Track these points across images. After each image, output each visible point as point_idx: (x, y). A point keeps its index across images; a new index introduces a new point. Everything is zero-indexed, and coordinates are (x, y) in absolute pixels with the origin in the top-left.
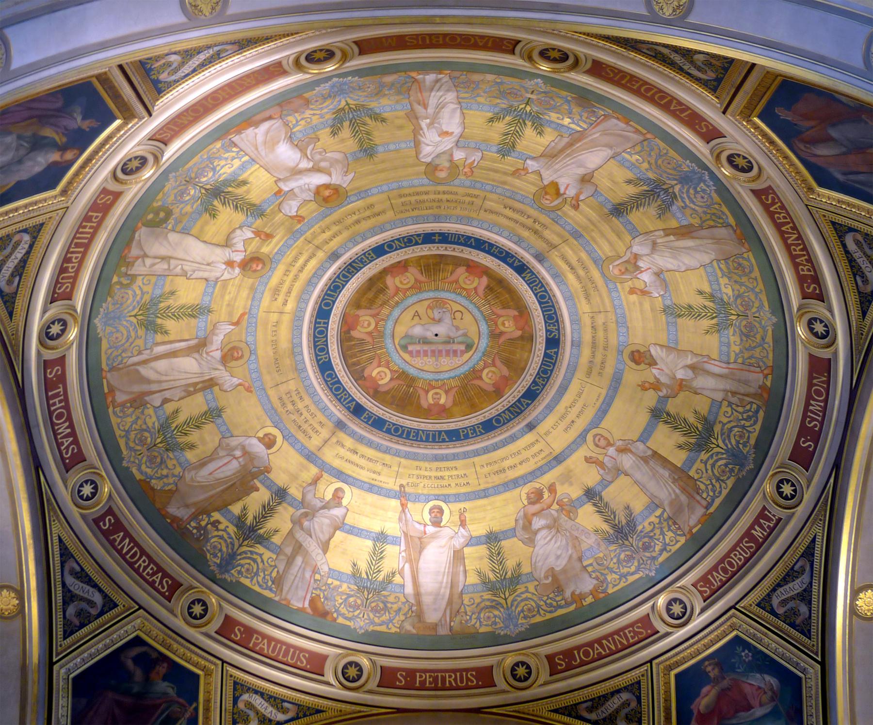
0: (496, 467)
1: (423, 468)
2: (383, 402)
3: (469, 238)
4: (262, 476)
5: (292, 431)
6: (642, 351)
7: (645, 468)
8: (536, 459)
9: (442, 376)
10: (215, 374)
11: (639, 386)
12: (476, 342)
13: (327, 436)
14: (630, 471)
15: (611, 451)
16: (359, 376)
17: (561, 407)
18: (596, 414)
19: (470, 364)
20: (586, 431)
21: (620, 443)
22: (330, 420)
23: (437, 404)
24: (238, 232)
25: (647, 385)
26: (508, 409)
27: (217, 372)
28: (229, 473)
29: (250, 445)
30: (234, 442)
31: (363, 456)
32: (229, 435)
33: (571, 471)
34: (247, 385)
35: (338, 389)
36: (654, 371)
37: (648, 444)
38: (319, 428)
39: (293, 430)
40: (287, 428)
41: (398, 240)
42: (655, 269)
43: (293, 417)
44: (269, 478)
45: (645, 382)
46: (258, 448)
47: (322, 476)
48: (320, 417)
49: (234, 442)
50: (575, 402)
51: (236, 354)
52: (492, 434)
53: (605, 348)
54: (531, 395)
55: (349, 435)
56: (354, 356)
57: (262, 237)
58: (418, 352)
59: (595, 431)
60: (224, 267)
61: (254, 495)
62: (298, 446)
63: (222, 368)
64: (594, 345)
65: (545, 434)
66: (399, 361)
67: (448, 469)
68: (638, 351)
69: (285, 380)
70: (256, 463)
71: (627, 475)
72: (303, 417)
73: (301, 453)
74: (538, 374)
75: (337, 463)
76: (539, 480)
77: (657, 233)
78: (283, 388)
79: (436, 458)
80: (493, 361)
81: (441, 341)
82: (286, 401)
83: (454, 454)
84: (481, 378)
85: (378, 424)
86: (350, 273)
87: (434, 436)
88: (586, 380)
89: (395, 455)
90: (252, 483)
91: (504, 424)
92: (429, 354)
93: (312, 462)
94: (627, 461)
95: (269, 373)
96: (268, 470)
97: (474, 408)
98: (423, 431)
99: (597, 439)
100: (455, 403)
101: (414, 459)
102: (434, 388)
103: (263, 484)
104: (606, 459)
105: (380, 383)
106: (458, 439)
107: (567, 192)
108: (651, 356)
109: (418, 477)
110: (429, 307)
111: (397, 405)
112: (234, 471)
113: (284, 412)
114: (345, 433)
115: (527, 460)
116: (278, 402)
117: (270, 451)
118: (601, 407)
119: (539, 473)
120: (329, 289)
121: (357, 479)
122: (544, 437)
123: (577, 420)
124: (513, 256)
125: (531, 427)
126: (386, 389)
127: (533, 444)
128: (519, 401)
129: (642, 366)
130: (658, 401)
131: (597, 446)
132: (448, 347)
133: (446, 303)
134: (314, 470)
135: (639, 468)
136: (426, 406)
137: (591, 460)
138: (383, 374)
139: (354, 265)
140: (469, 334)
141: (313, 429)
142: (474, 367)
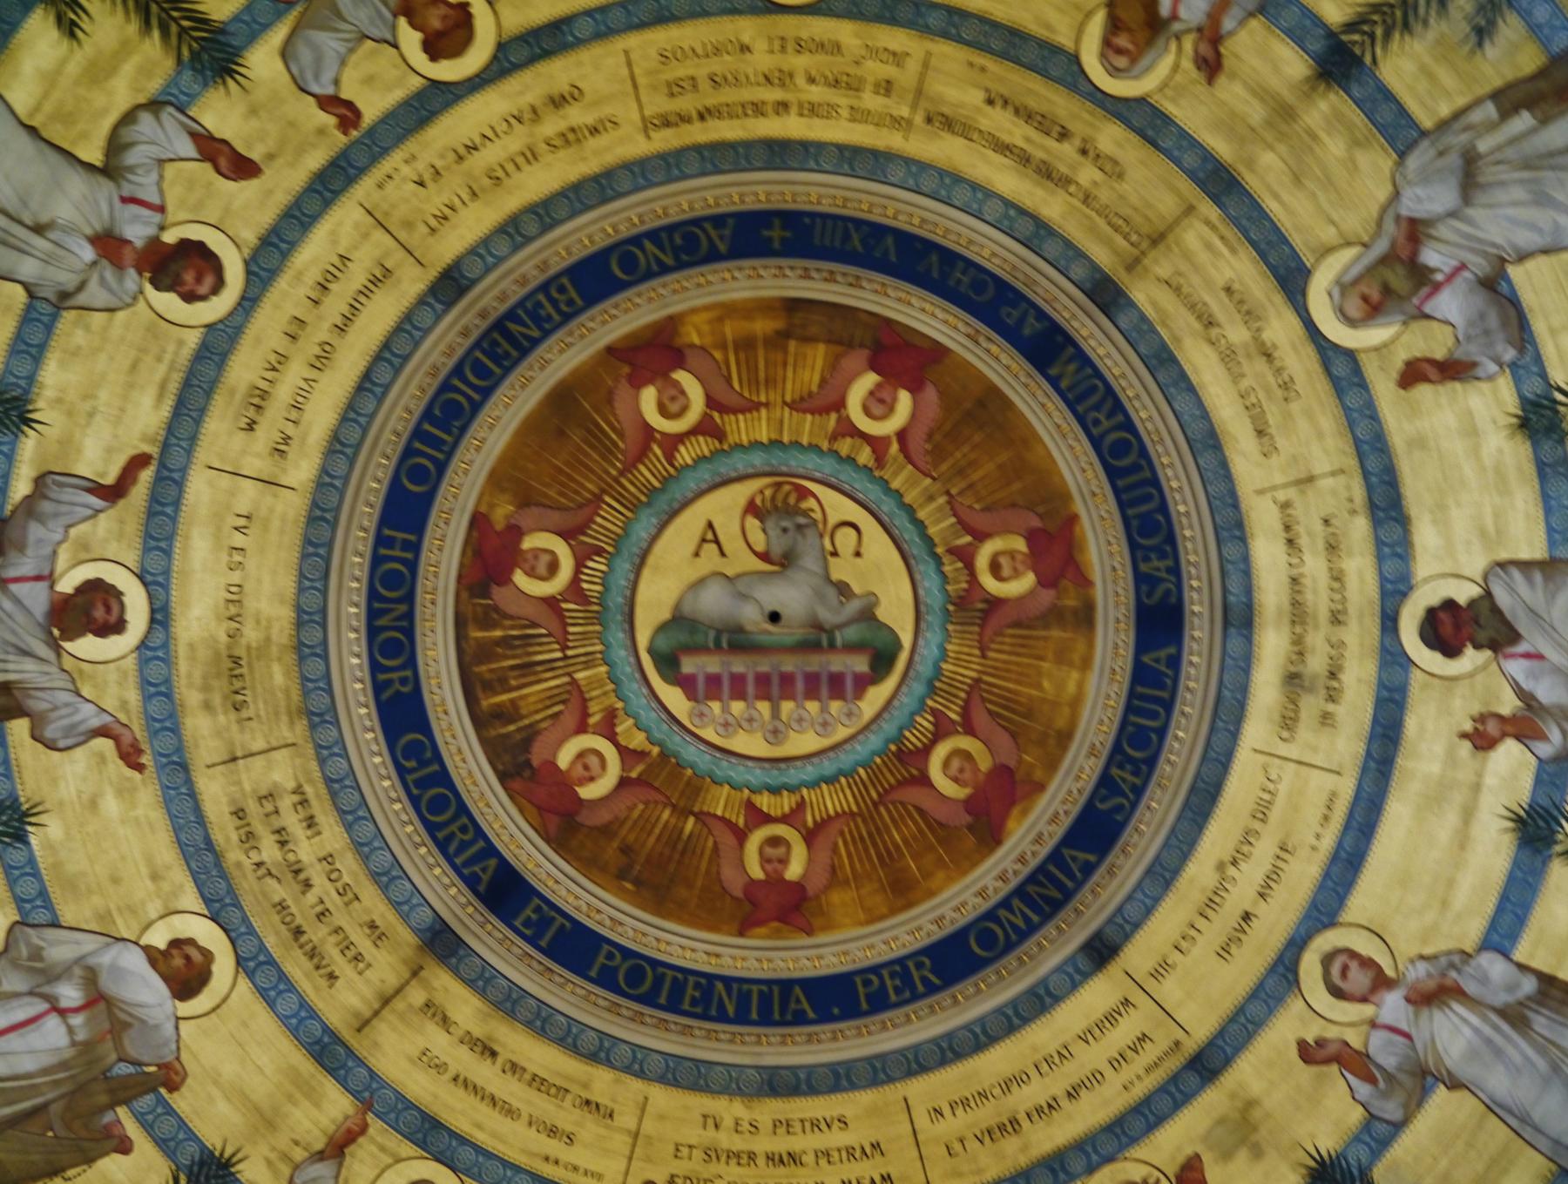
0: (986, 1115)
1: (728, 1122)
2: (589, 864)
3: (878, 231)
4: (149, 1099)
5: (270, 942)
6: (1462, 600)
7: (1518, 1048)
8: (1127, 1072)
9: (794, 775)
10: (22, 670)
11: (1464, 736)
12: (906, 639)
13: (393, 981)
14: (1464, 1072)
15: (1393, 1006)
16: (518, 765)
17: (1199, 871)
18: (1327, 875)
19: (889, 728)
20: (1296, 945)
21: (1422, 969)
22: (405, 918)
23: (775, 882)
24: (146, 120)
25: (1492, 728)
26: (1019, 892)
27: (29, 665)
28: (28, 1065)
29: (115, 969)
30: (60, 949)
31: (514, 1068)
32: (41, 916)
33: (1251, 1104)
34: (126, 739)
35: (438, 805)
36: (1516, 668)
37: (1520, 955)
38: (363, 943)
39: (273, 939)
40: (251, 931)
41: (653, 235)
42: (1480, 265)
43: (278, 892)
44: (170, 1111)
45: (1481, 719)
46: (145, 990)
47: (363, 1129)
48: (373, 903)
49: (60, 949)
50: (1248, 837)
51: (99, 613)
52: (967, 986)
53: (1337, 619)
54: (1096, 830)
55: (470, 983)
56: (499, 683)
57: (223, 162)
58: (714, 681)
59: (1326, 941)
60: (88, 253)
61: (111, 1164)
62: (288, 1004)
63: (43, 650)
64: (1298, 613)
65: (1156, 975)
66: (650, 716)
67: (815, 1125)
68: (1450, 605)
69: (259, 744)
70: (132, 1051)
71: (1454, 1084)
72: (311, 897)
73: (295, 1032)
74: (1117, 748)
75: (420, 1087)
76: (1138, 1152)
77: (1476, 116)
78: (255, 775)
79: (779, 1083)
80: (966, 712)
81: (789, 640)
82: (259, 828)
83: (833, 1067)
84: (924, 781)
85: (573, 947)
86: (497, 360)
87: (765, 999)
88: (1283, 749)
89: (627, 1070)
90: (108, 1118)
91: (1009, 947)
92: (751, 689)
93: (331, 1072)
94: (1452, 1034)
95: (207, 706)
96: (171, 1077)
97: (903, 891)
98: (727, 981)
99: (1335, 970)
100: (835, 877)
101: (694, 1087)
102: (767, 819)
103: (147, 1127)
104: (1378, 1040)
105: (588, 792)
106: (851, 1011)
107: (1183, 12)
108: (1496, 611)
109: (711, 1154)
110: (752, 508)
111: (637, 882)
112: (47, 1060)
113: (247, 863)
114: (456, 972)
115: (1096, 1077)
116: (231, 823)
117: (185, 1008)
118: (1340, 844)
119: (1138, 1124)
120: (427, 415)
121: (489, 1155)
122: (1150, 985)
123: (1261, 909)
124: (1021, 297)
125: (1100, 952)
126: (604, 816)
127: (1111, 1018)
128: (1055, 856)
129: (1471, 658)
130: (1538, 781)
131: (1337, 993)
132: (814, 663)
133: (804, 493)
134: (337, 1104)
135: (1498, 1053)
136: (738, 893)
137: (1323, 1053)
138: (593, 761)
139: (512, 326)
140: (882, 614)
141: (346, 946)
142: (899, 739)
